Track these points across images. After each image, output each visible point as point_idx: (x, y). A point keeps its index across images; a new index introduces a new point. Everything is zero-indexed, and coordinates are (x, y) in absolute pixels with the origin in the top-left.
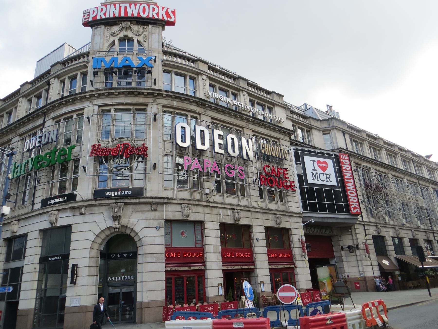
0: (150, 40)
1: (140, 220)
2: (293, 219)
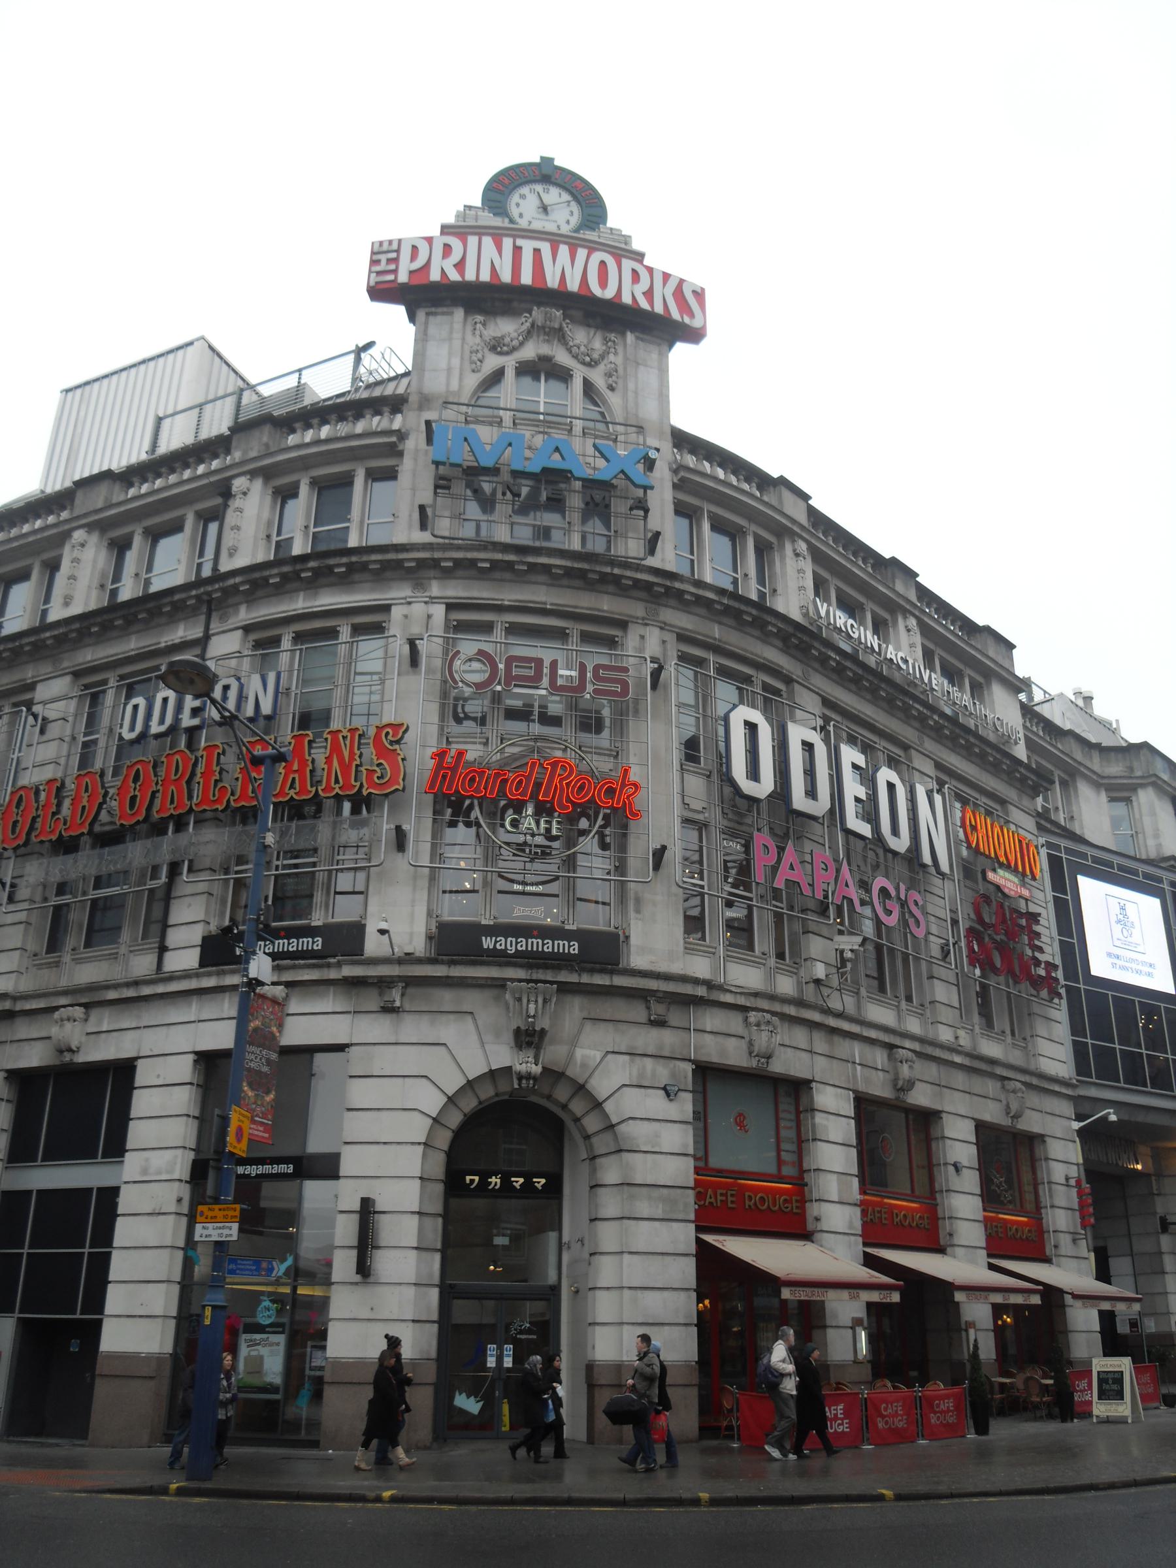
0: (631, 386)
1: (610, 1056)
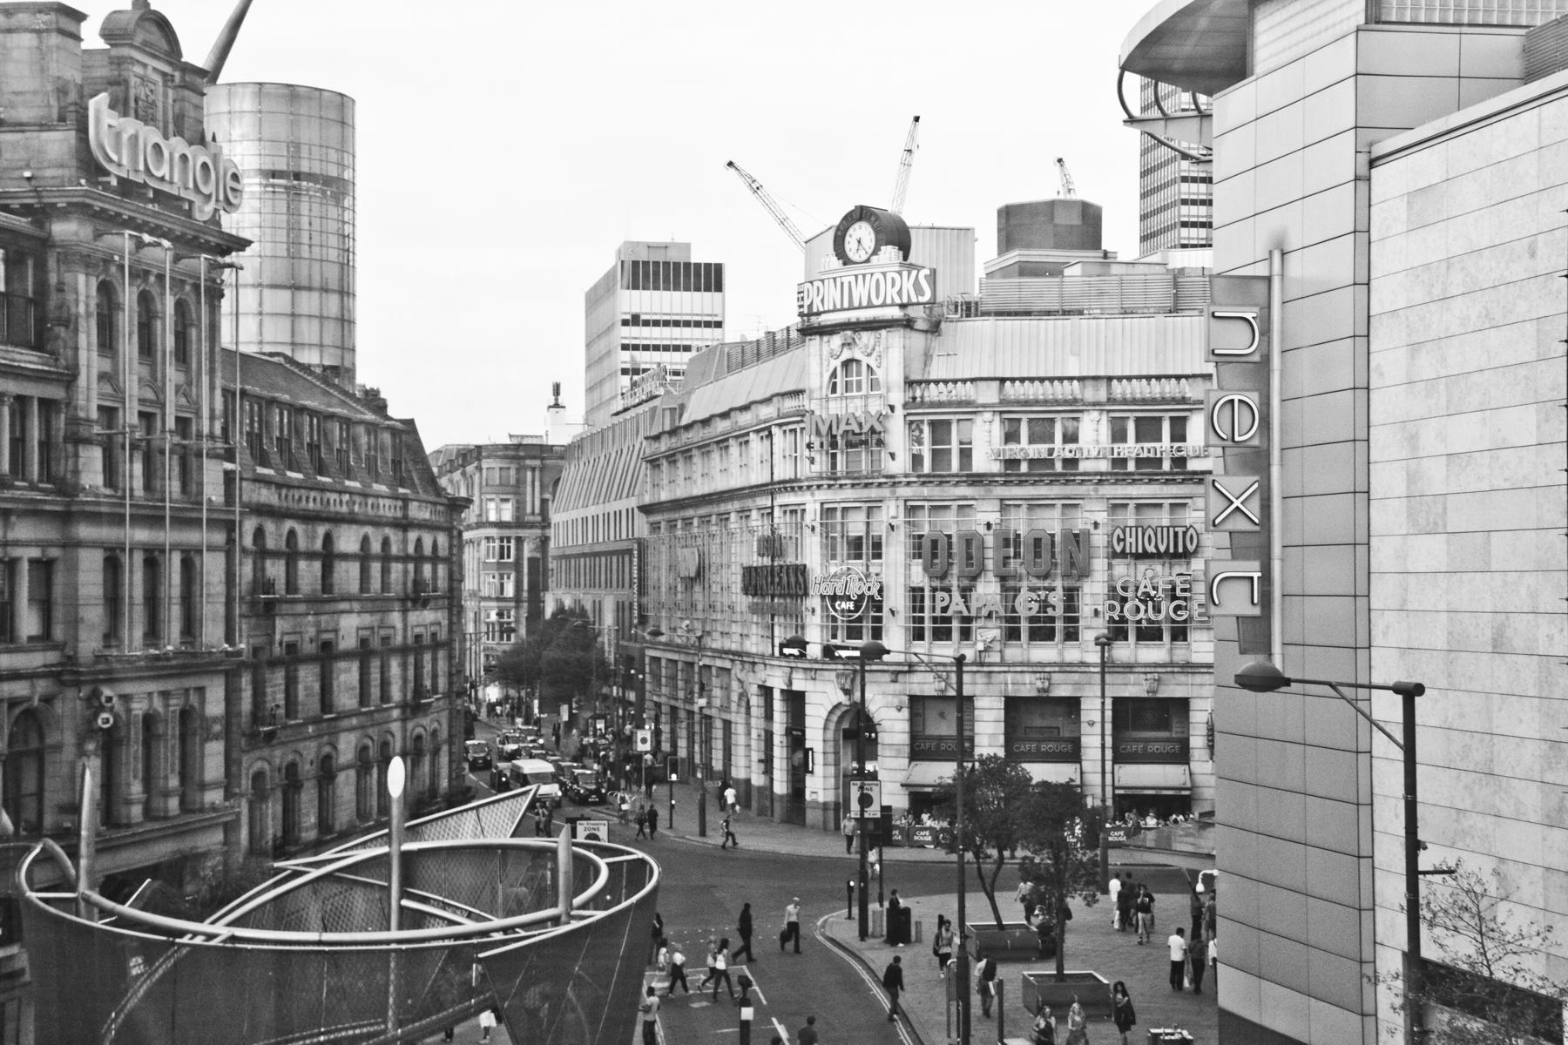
2: (1198, 679)
